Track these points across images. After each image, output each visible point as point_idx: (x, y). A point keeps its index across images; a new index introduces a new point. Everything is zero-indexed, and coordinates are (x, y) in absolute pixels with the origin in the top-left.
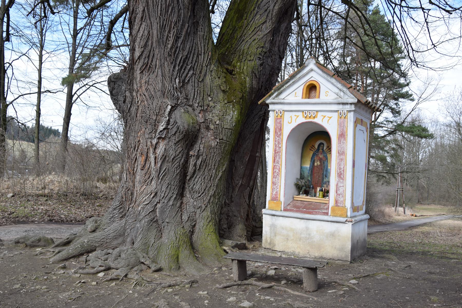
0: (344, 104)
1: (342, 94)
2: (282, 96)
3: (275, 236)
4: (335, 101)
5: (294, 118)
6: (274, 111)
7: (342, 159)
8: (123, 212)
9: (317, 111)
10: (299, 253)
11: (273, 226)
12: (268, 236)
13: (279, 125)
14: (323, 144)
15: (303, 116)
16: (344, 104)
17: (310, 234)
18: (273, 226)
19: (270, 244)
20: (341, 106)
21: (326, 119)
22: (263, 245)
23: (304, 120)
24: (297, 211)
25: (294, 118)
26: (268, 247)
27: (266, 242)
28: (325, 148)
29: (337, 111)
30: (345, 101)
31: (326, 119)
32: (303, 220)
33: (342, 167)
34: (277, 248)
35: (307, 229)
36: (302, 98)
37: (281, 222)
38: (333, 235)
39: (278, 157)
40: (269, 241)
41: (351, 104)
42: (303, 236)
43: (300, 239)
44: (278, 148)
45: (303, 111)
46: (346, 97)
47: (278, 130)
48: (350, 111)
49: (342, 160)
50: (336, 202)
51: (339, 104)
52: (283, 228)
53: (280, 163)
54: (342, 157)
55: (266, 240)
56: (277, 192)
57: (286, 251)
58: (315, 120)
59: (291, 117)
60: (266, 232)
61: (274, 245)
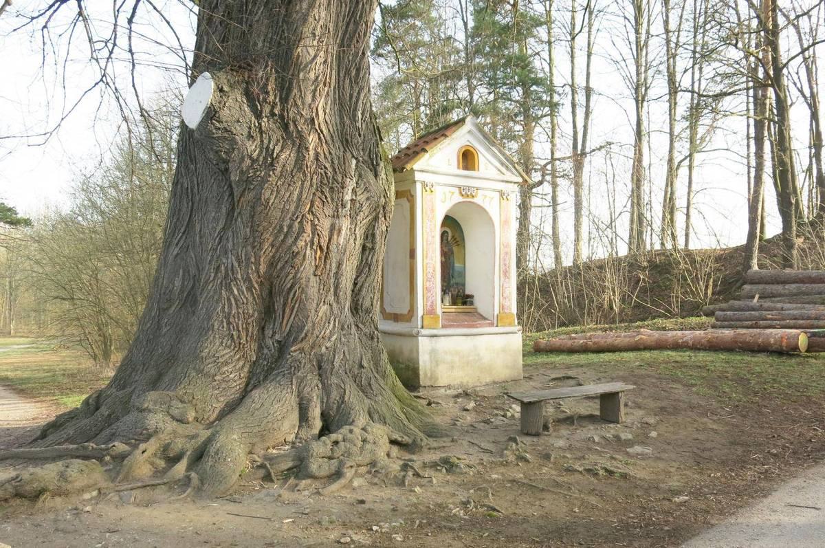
1: (503, 170)
3: (437, 365)
5: (448, 195)
8: (243, 367)
10: (468, 382)
11: (433, 352)
12: (428, 367)
14: (447, 232)
17: (479, 355)
18: (433, 352)
19: (431, 378)
22: (421, 383)
23: (461, 199)
24: (458, 326)
26: (428, 383)
28: (449, 238)
32: (469, 337)
33: (507, 263)
34: (442, 382)
36: (458, 168)
37: (444, 344)
39: (431, 250)
40: (429, 375)
41: (515, 183)
42: (471, 358)
44: (430, 238)
51: (503, 181)
52: (446, 353)
53: (434, 259)
55: (426, 375)
56: (432, 302)
58: (475, 200)
59: (444, 193)
61: (437, 379)
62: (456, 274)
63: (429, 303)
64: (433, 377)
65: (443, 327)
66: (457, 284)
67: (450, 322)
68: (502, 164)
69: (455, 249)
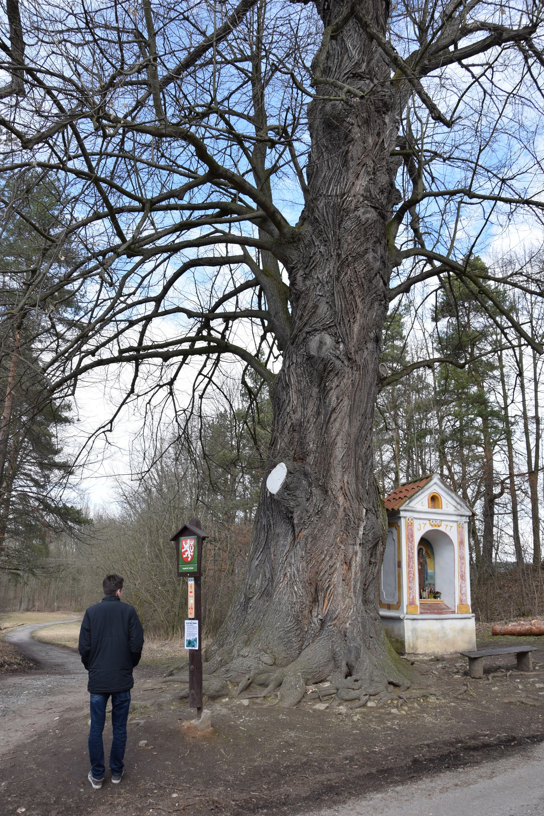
0: (461, 516)
1: (459, 507)
2: (412, 504)
4: (457, 513)
5: (422, 525)
6: (405, 517)
7: (462, 563)
9: (442, 521)
11: (414, 630)
12: (411, 641)
13: (410, 531)
15: (430, 524)
16: (461, 516)
17: (445, 633)
18: (414, 630)
19: (413, 648)
20: (459, 518)
21: (449, 528)
24: (431, 613)
25: (422, 525)
26: (411, 651)
27: (409, 647)
29: (457, 522)
30: (463, 514)
31: (449, 528)
34: (420, 651)
35: (443, 628)
37: (421, 625)
38: (462, 630)
43: (438, 639)
45: (429, 520)
46: (463, 510)
47: (410, 536)
48: (465, 522)
49: (462, 563)
50: (461, 600)
54: (462, 561)
55: (409, 645)
57: (427, 652)
58: (440, 529)
60: (408, 637)
61: (417, 649)
62: (429, 577)
63: (411, 597)
64: (414, 647)
65: (421, 613)
66: (430, 584)
67: (427, 609)
68: (458, 504)
69: (428, 560)
